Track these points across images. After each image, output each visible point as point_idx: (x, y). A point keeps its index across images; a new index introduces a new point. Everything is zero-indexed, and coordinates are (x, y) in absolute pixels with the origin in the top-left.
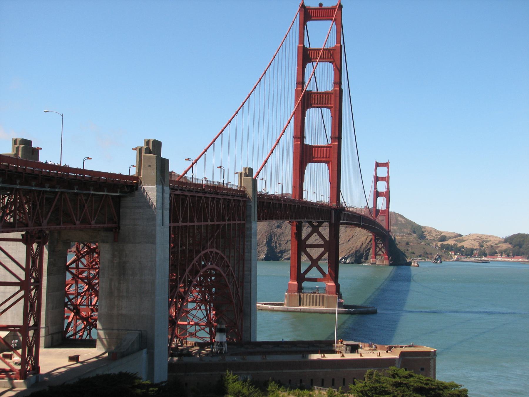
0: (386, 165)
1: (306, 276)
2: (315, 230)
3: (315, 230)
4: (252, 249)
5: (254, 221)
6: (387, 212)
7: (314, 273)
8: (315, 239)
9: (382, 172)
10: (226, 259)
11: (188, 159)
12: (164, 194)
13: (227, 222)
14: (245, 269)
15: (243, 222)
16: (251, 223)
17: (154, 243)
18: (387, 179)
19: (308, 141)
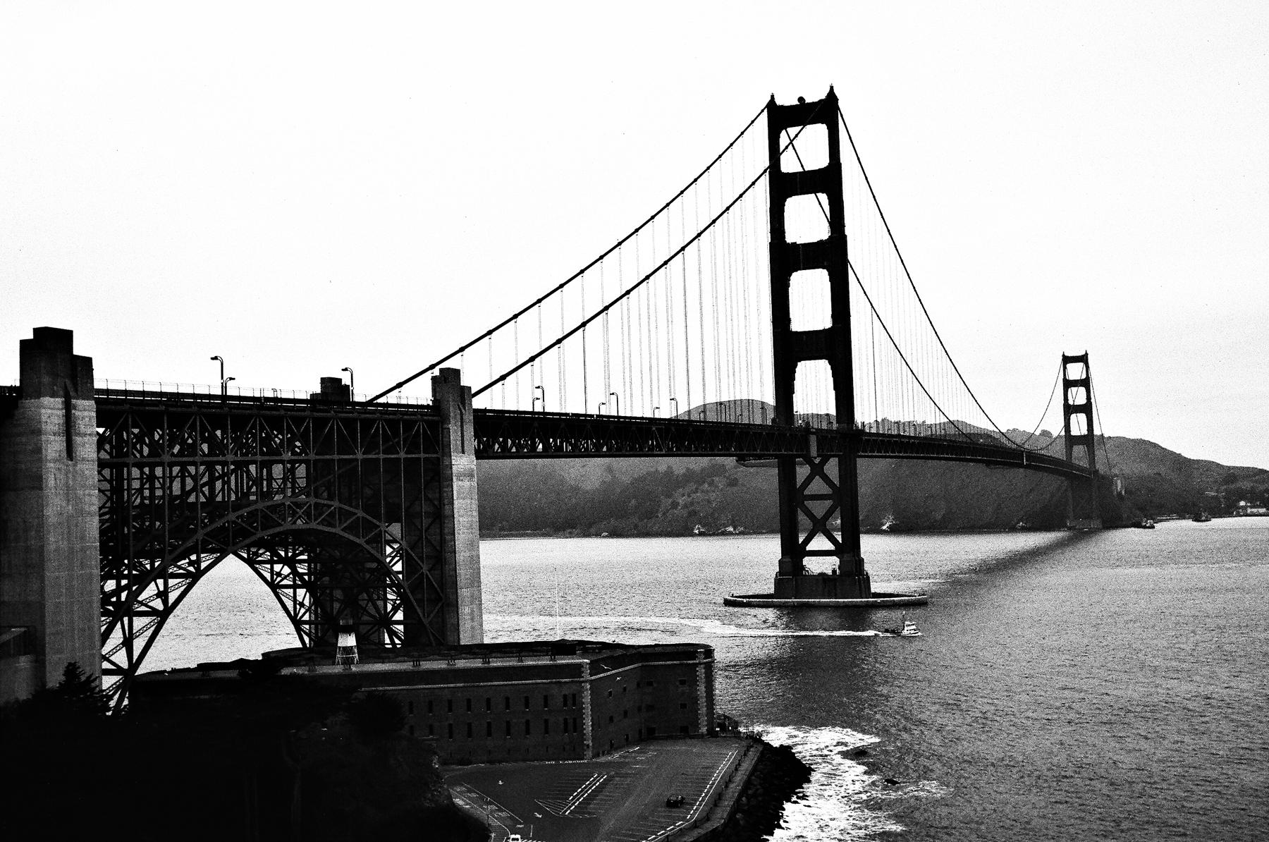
0: (1083, 359)
1: (809, 547)
2: (817, 471)
3: (817, 471)
4: (455, 498)
5: (463, 452)
6: (1089, 440)
7: (820, 543)
8: (817, 486)
9: (1076, 371)
10: (360, 514)
11: (216, 358)
12: (73, 411)
13: (360, 456)
14: (446, 531)
15: (435, 456)
16: (451, 456)
17: (41, 489)
18: (1085, 383)
19: (799, 323)
